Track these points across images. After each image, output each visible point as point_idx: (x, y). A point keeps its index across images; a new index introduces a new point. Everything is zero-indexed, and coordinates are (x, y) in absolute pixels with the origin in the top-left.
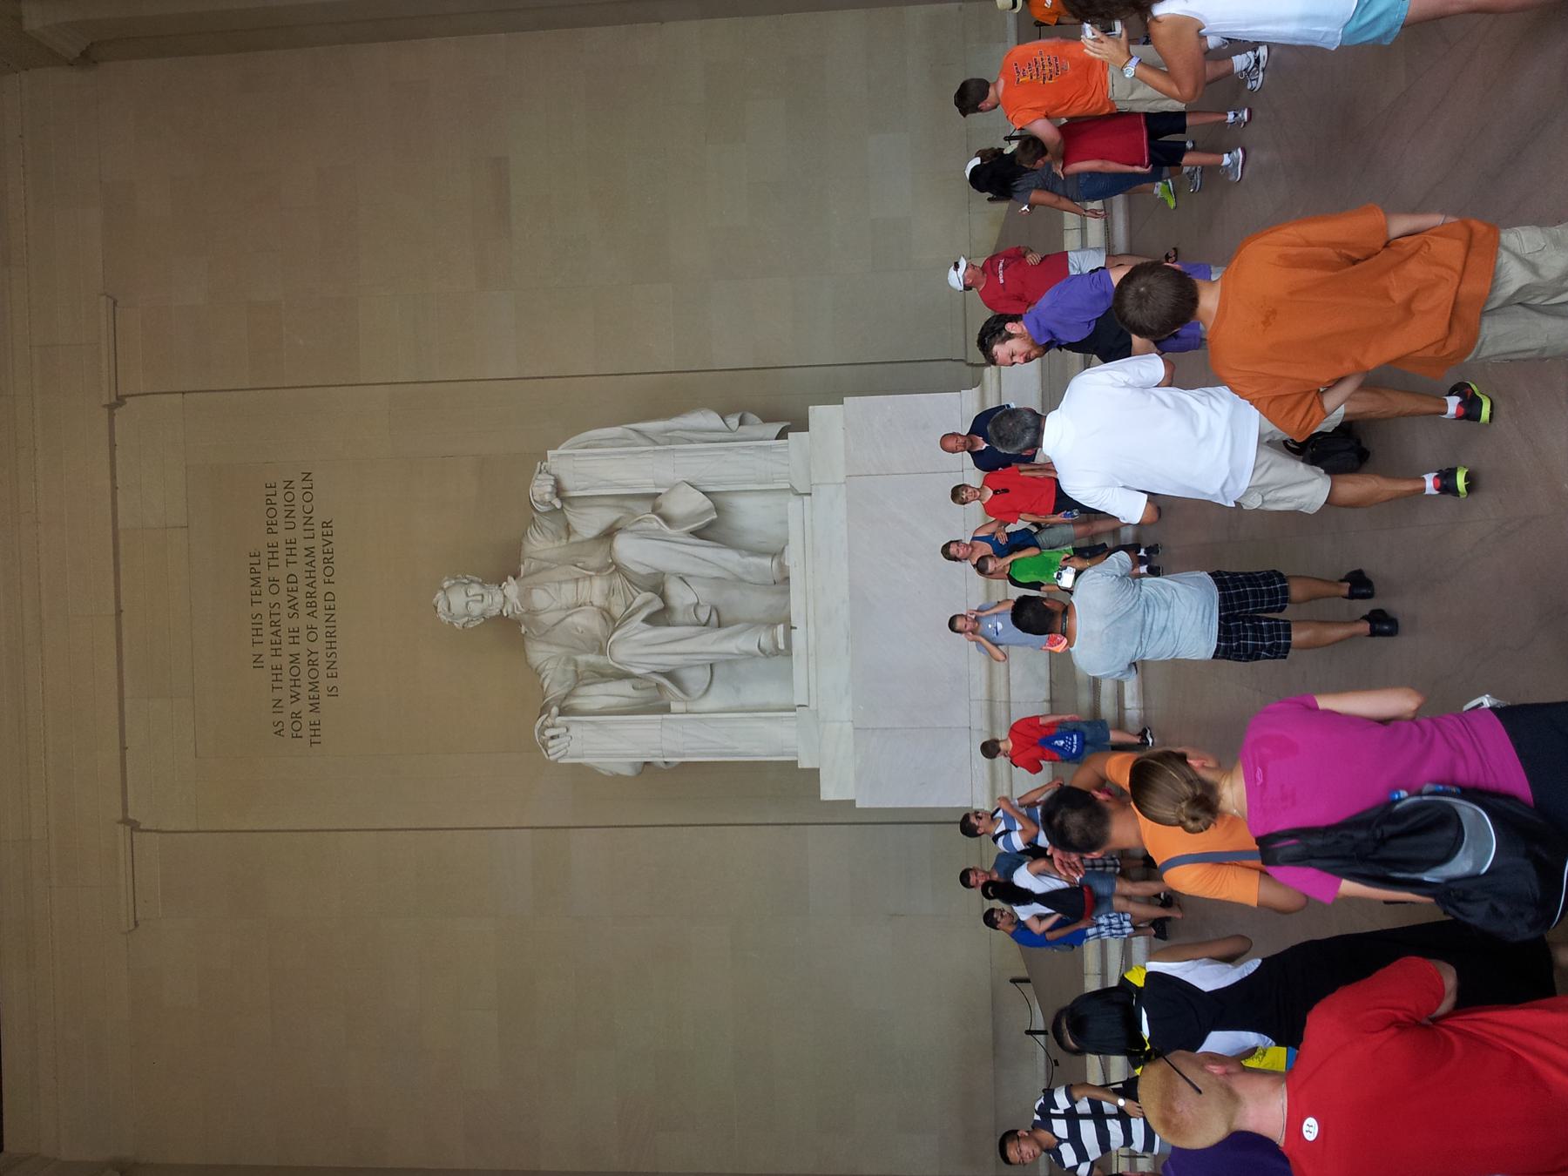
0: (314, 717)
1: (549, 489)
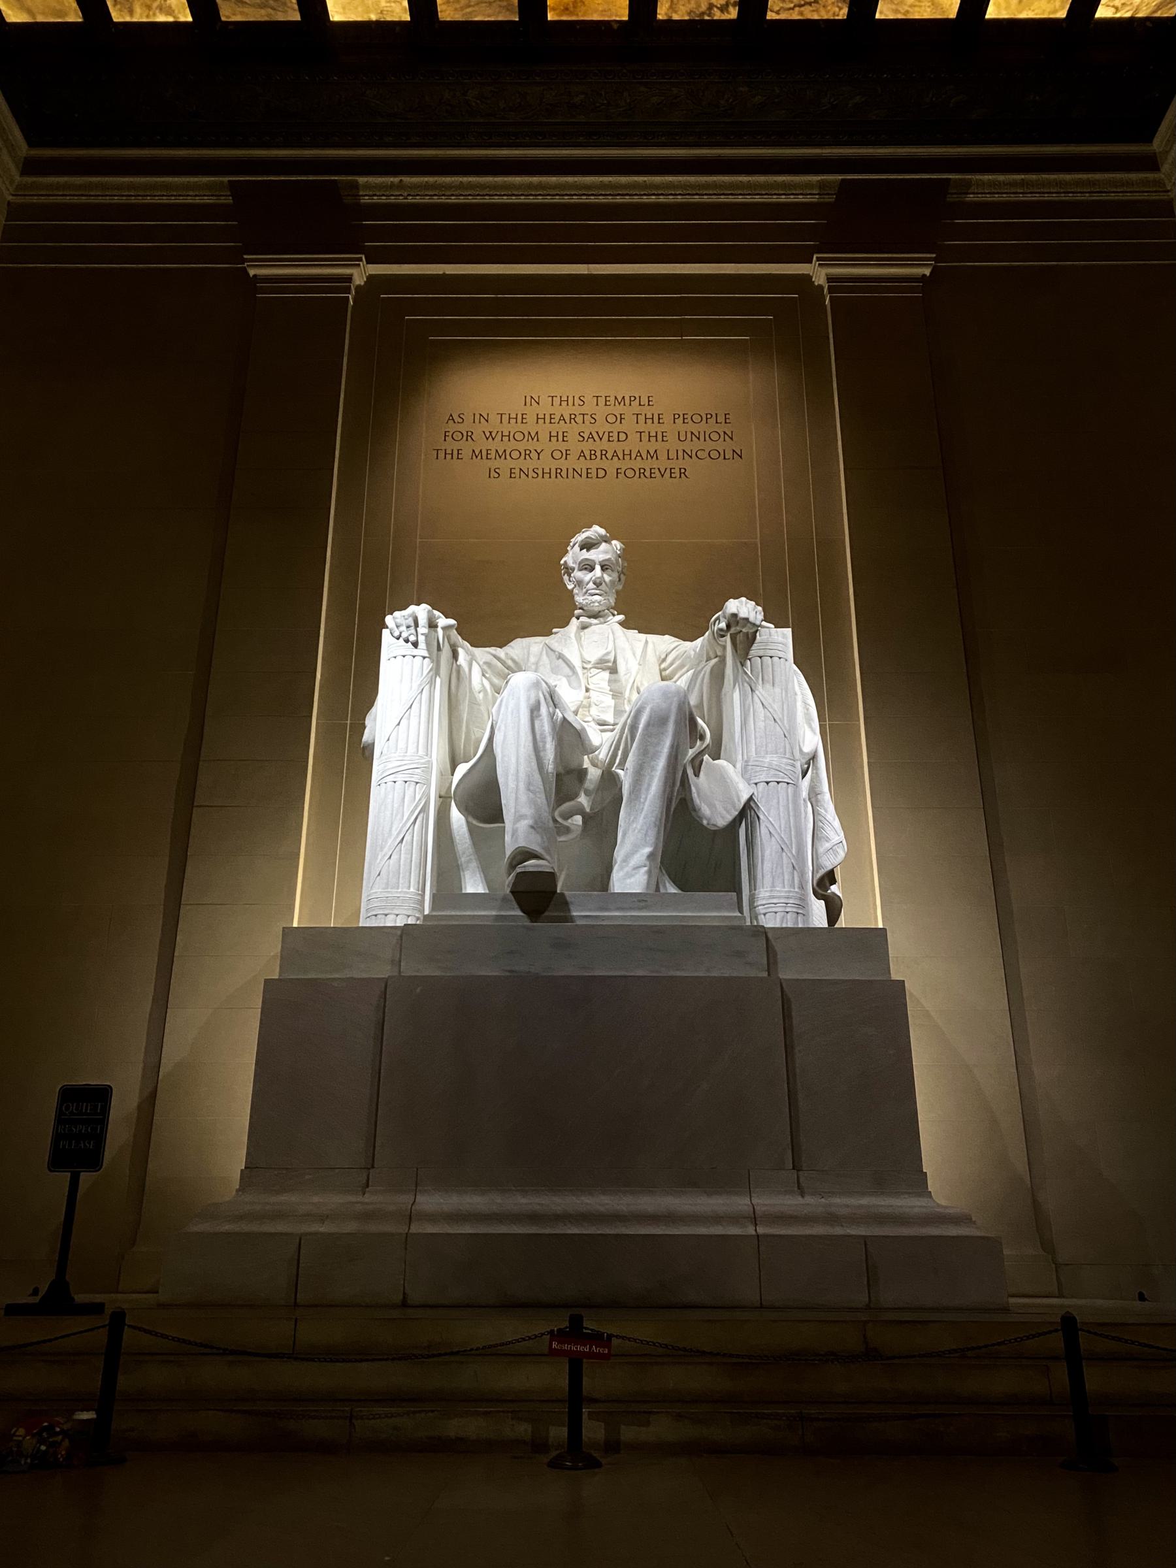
0: (466, 453)
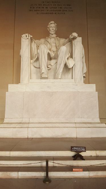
1: (75, 35)
